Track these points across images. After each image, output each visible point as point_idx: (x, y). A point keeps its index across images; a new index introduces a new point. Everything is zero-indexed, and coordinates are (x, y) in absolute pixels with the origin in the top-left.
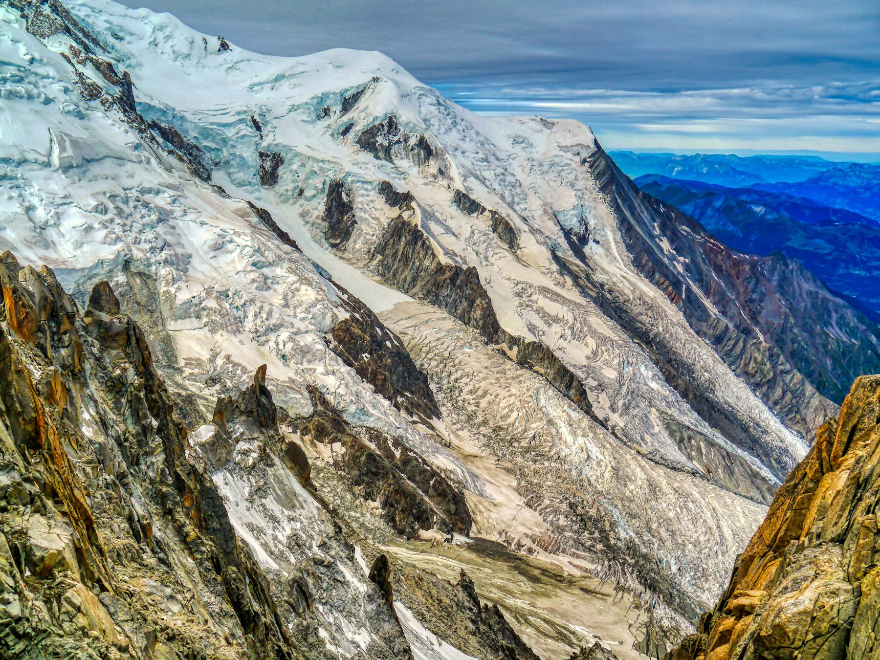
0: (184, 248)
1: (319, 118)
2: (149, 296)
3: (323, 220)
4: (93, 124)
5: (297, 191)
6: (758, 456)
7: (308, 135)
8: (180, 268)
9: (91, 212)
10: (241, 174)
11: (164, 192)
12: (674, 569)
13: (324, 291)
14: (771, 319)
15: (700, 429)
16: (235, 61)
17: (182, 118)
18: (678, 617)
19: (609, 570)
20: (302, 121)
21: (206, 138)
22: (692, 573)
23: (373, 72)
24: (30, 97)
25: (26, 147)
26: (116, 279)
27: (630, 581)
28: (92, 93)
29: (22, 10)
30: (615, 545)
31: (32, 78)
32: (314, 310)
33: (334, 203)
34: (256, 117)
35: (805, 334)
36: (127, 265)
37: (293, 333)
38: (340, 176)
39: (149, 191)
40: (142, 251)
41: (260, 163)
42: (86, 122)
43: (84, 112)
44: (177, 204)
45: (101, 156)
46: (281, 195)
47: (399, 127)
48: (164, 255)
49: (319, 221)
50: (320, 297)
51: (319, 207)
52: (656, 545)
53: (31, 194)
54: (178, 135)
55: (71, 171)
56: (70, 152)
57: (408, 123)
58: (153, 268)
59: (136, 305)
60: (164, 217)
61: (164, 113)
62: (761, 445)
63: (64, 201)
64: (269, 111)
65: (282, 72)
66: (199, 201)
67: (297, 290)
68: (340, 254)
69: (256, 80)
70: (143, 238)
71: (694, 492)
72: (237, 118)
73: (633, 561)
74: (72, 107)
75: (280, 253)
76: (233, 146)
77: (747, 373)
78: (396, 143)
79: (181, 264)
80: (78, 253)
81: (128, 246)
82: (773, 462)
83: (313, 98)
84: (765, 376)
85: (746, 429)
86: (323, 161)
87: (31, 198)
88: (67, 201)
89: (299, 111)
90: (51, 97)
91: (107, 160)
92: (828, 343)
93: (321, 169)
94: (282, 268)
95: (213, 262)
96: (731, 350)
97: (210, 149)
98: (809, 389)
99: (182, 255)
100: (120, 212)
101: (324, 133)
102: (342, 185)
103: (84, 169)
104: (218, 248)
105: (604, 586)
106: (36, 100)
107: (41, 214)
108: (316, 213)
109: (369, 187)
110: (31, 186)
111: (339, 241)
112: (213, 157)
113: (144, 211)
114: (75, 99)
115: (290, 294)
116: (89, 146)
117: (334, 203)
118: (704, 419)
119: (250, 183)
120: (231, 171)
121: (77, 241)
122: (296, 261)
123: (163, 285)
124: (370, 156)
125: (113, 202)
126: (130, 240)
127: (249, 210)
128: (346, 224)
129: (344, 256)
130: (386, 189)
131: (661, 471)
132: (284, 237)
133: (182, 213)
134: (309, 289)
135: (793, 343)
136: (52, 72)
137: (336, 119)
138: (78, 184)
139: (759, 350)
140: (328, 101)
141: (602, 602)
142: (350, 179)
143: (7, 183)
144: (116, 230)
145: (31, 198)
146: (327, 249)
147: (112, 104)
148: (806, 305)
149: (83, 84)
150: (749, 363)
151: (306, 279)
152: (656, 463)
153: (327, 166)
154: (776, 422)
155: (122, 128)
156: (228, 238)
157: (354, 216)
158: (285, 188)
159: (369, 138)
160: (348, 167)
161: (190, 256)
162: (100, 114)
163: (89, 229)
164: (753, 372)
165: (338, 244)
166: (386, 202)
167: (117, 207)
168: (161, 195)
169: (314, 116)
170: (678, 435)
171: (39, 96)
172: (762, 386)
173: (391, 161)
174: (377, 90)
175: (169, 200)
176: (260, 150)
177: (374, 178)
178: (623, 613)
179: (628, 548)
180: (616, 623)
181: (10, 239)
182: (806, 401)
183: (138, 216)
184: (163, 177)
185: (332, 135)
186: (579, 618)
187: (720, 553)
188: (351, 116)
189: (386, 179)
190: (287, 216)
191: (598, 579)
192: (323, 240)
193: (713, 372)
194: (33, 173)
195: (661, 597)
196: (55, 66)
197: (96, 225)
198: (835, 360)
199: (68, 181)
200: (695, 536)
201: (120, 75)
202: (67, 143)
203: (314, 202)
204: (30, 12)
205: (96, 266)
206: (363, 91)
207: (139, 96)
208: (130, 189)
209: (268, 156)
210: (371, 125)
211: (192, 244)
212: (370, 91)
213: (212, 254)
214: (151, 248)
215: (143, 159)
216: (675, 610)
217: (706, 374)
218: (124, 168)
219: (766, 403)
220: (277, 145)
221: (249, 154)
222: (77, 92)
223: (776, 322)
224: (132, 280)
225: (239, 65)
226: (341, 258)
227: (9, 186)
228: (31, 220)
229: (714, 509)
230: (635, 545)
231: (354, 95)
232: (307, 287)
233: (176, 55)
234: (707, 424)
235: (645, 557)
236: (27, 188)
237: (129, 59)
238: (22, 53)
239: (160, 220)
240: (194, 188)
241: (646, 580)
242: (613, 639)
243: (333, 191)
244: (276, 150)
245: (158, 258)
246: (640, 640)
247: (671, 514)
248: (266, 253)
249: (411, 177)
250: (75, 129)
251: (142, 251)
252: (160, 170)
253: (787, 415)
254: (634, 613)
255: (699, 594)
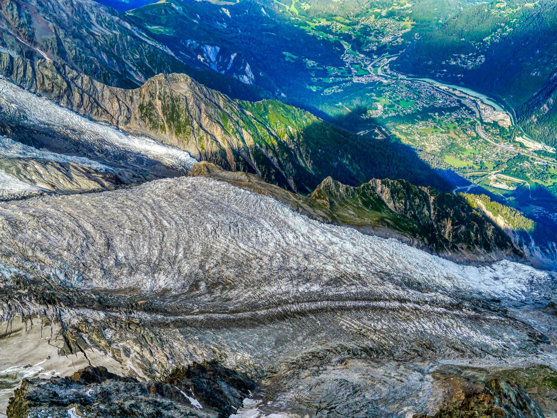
6: (85, 155)
12: (62, 277)
14: (43, 37)
15: (29, 155)
18: (82, 311)
19: (11, 309)
22: (77, 272)
27: (32, 308)
30: (5, 287)
35: (77, 40)
52: (39, 267)
62: (83, 145)
71: (48, 209)
73: (26, 291)
77: (45, 91)
82: (98, 154)
84: (61, 88)
85: (66, 138)
92: (97, 41)
96: (24, 76)
98: (99, 85)
105: (13, 324)
118: (30, 145)
131: (13, 205)
135: (71, 51)
139: (46, 68)
141: (17, 337)
148: (67, 15)
150: (43, 82)
152: (6, 201)
154: (86, 122)
164: (50, 88)
170: (13, 168)
172: (62, 97)
178: (39, 334)
179: (18, 283)
180: (37, 346)
182: (100, 95)
186: (4, 362)
187: (90, 245)
191: (6, 322)
193: (18, 101)
195: (62, 304)
198: (106, 52)
200: (65, 243)
216: (77, 307)
217: (13, 105)
219: (71, 110)
223: (50, 37)
229: (69, 214)
230: (21, 277)
234: (33, 148)
235: (34, 282)
241: (44, 299)
242: (41, 359)
246: (62, 346)
247: (39, 237)
253: (91, 112)
254: (47, 331)
255: (89, 284)
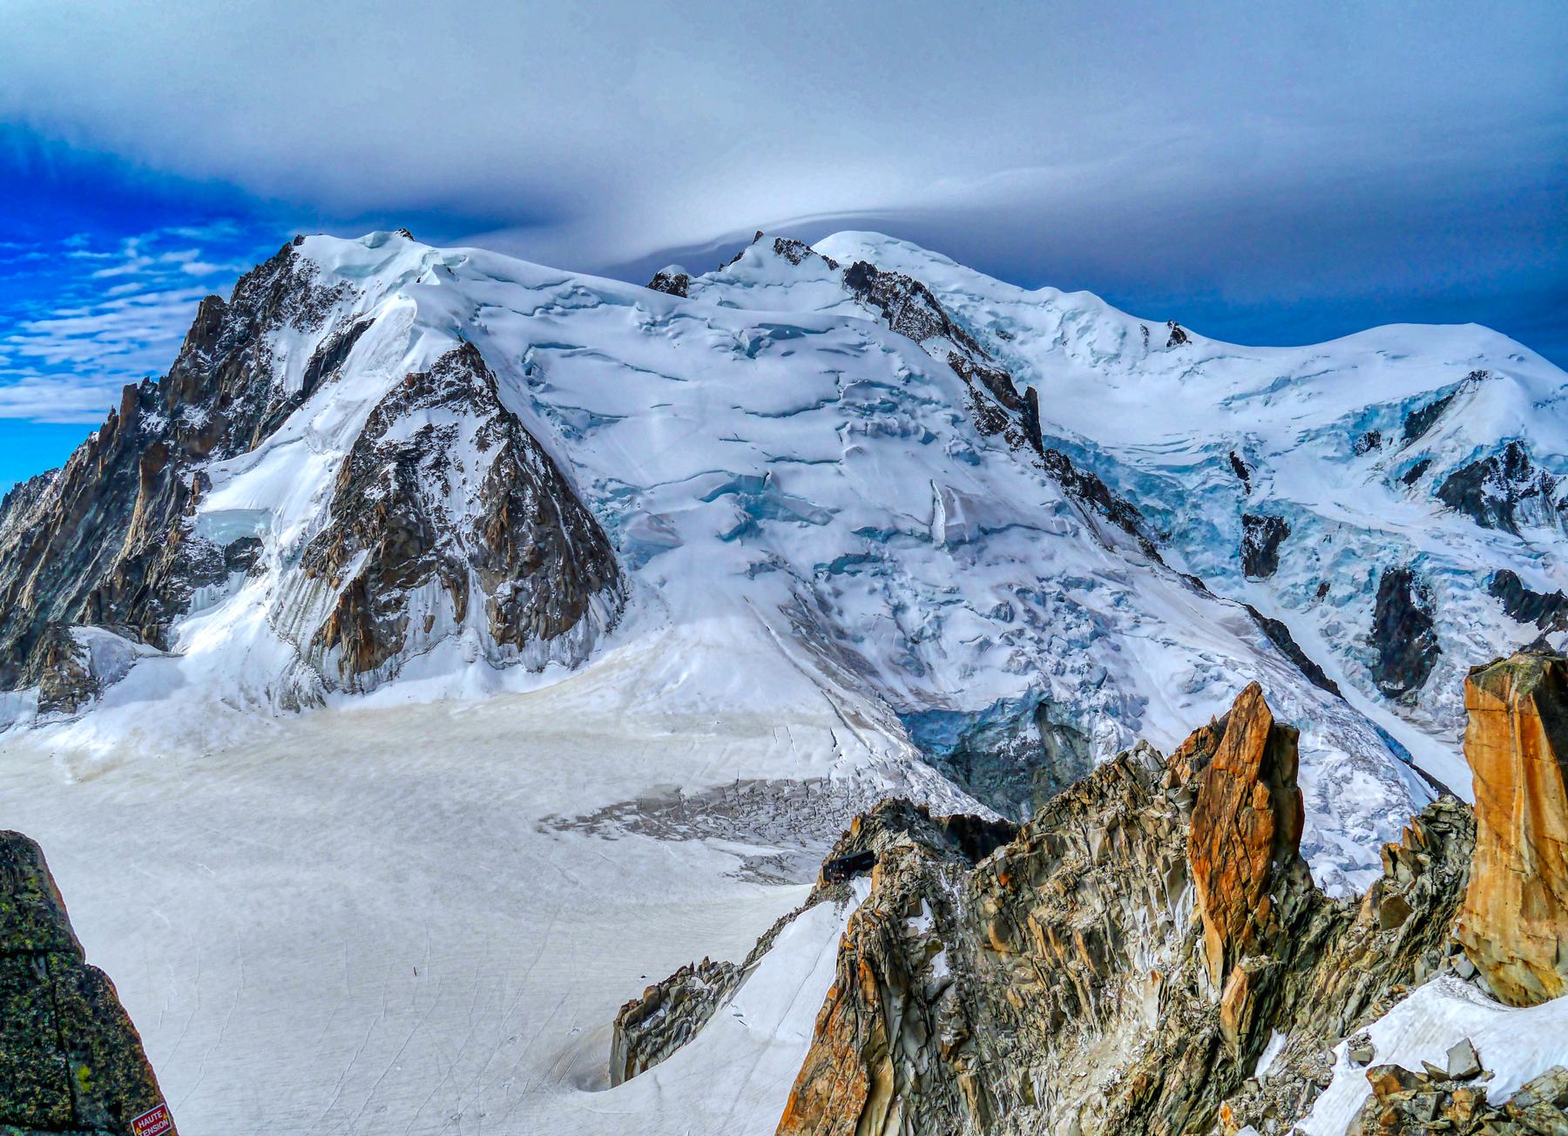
0: (1134, 686)
1: (1357, 451)
2: (1075, 769)
3: (1369, 642)
4: (992, 472)
5: (1316, 587)
7: (1337, 484)
8: (1128, 721)
9: (988, 617)
10: (1208, 555)
11: (1101, 585)
13: (1403, 787)
16: (1196, 360)
17: (1110, 460)
20: (1325, 458)
21: (1147, 493)
23: (1470, 362)
24: (905, 433)
25: (899, 512)
26: (1022, 734)
28: (993, 424)
29: (885, 306)
31: (908, 405)
32: (1381, 823)
33: (1393, 612)
34: (1239, 454)
36: (1041, 710)
37: (1340, 865)
38: (1404, 561)
39: (1078, 583)
40: (1068, 687)
41: (1243, 534)
42: (981, 470)
43: (979, 453)
44: (1123, 606)
45: (1003, 525)
46: (1284, 594)
47: (1532, 463)
48: (1103, 696)
49: (1362, 645)
50: (1394, 799)
51: (1361, 618)
53: (902, 585)
54: (1103, 489)
55: (962, 548)
56: (960, 519)
57: (1551, 456)
58: (1085, 719)
59: (1052, 784)
60: (1102, 629)
61: (1081, 451)
63: (949, 597)
64: (1262, 442)
65: (1285, 374)
66: (1160, 604)
67: (1347, 780)
68: (1405, 711)
69: (1236, 391)
70: (1069, 665)
72: (1205, 456)
74: (963, 447)
75: (1313, 705)
76: (1196, 506)
78: (1524, 495)
79: (1130, 710)
80: (966, 685)
81: (1046, 679)
83: (1347, 416)
86: (1369, 531)
87: (900, 592)
88: (953, 597)
89: (1319, 441)
90: (933, 431)
91: (1015, 530)
93: (1366, 547)
94: (1315, 734)
95: (1184, 712)
97: (1153, 511)
99: (1132, 698)
100: (1033, 619)
101: (1370, 479)
102: (1410, 578)
103: (980, 544)
104: (1195, 688)
106: (913, 438)
107: (914, 618)
108: (1354, 630)
109: (1468, 582)
110: (902, 572)
111: (1401, 686)
112: (1159, 524)
113: (1069, 618)
114: (967, 435)
115: (1332, 788)
116: (989, 508)
117: (1393, 612)
119: (1224, 572)
120: (1190, 549)
121: (965, 666)
122: (1343, 723)
123: (1101, 749)
124: (1468, 522)
125: (1023, 600)
126: (1049, 666)
127: (1249, 620)
128: (1418, 653)
129: (1413, 716)
130: (1506, 587)
132: (1314, 673)
133: (1132, 623)
134: (1371, 779)
136: (935, 393)
137: (1394, 453)
138: (971, 570)
140: (1377, 422)
142: (1426, 566)
143: (869, 568)
144: (1026, 649)
145: (900, 592)
146: (1376, 700)
147: (1022, 439)
149: (980, 409)
151: (1364, 759)
153: (1376, 540)
155: (1037, 479)
156: (1213, 672)
157: (1435, 638)
158: (1291, 581)
159: (1464, 488)
160: (1421, 543)
161: (1145, 702)
162: (1003, 457)
163: (985, 645)
165: (1401, 692)
166: (1507, 611)
167: (1029, 608)
168: (1096, 591)
169: (1347, 449)
171: (917, 430)
173: (1514, 530)
174: (1480, 394)
175: (1111, 600)
176: (1244, 512)
177: (1479, 563)
181: (870, 659)
183: (1060, 625)
184: (1101, 561)
185: (1386, 482)
188: (1425, 447)
189: (1506, 565)
190: (1306, 630)
192: (1369, 684)
194: (906, 552)
196: (942, 383)
197: (996, 640)
199: (957, 564)
201: (1022, 393)
202: (957, 504)
203: (1351, 609)
204: (895, 308)
205: (993, 709)
206: (1449, 399)
207: (1046, 430)
208: (1047, 580)
209: (1259, 522)
210: (1470, 463)
211: (1149, 680)
212: (1466, 397)
213: (1184, 699)
214: (1082, 684)
215: (1068, 528)
218: (1039, 545)
220: (1276, 503)
221: (1225, 519)
222: (971, 422)
224: (1049, 738)
225: (1205, 366)
226: (1406, 719)
227: (872, 571)
228: (899, 627)
231: (1430, 407)
232: (1366, 775)
233: (1097, 357)
236: (896, 576)
237: (1021, 367)
238: (896, 368)
239: (1096, 635)
240: (1149, 580)
243: (1391, 587)
244: (1276, 512)
245: (1094, 702)
248: (1285, 704)
249: (1561, 563)
250: (967, 481)
251: (1068, 687)
252: (1095, 548)
